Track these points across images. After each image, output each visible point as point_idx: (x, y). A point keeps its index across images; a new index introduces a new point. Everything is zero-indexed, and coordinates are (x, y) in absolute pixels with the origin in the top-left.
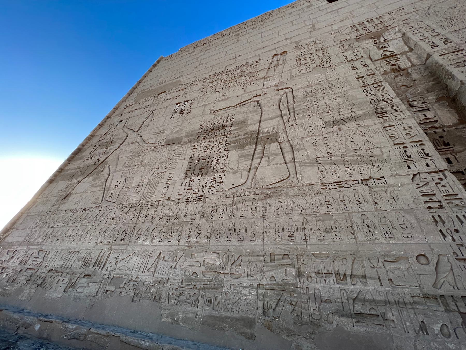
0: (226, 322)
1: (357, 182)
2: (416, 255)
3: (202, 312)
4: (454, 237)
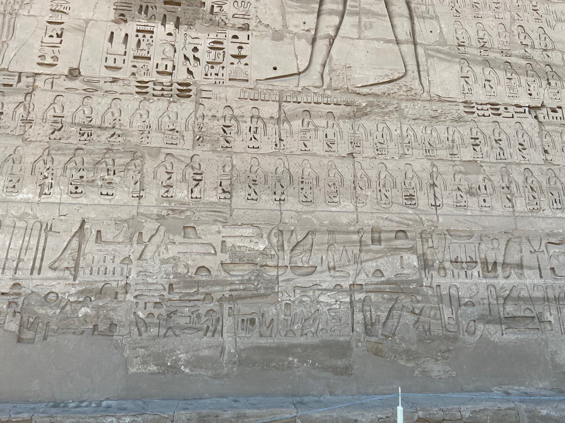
0: (293, 355)
1: (522, 110)
3: (236, 342)
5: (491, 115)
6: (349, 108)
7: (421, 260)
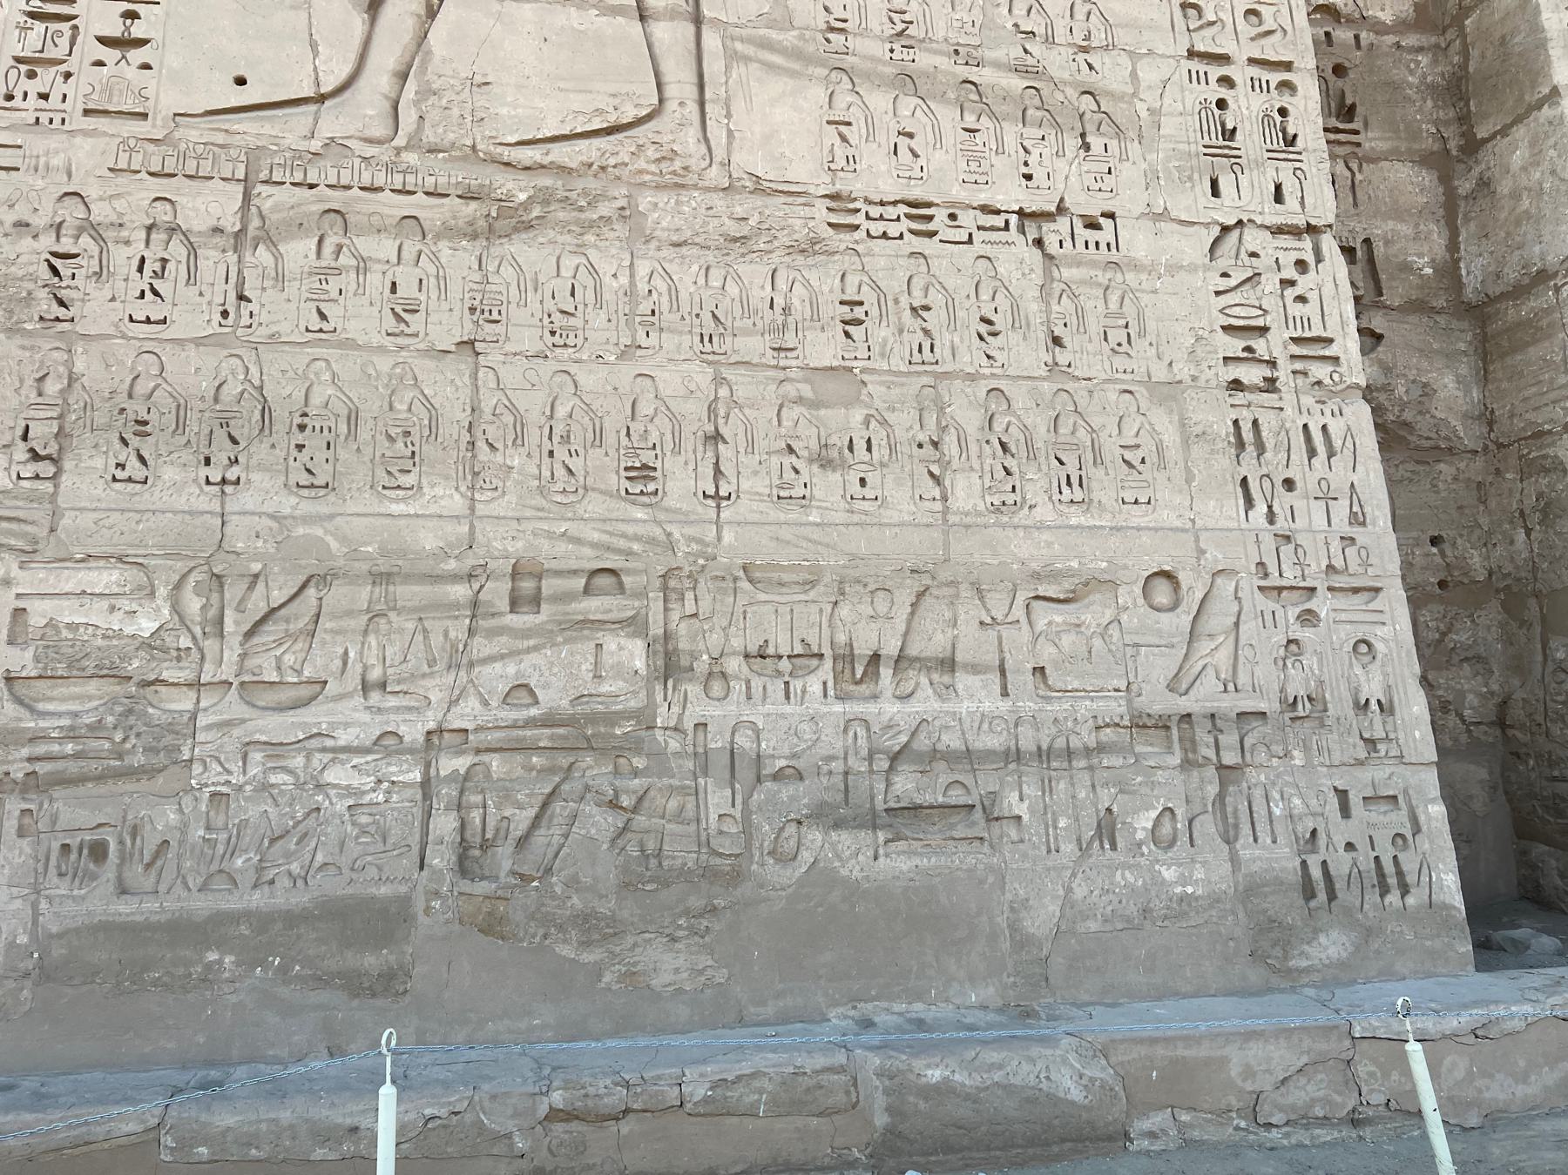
0: (222, 945)
1: (998, 221)
2: (1147, 574)
4: (1276, 508)
5: (907, 235)
6: (473, 205)
7: (655, 653)
